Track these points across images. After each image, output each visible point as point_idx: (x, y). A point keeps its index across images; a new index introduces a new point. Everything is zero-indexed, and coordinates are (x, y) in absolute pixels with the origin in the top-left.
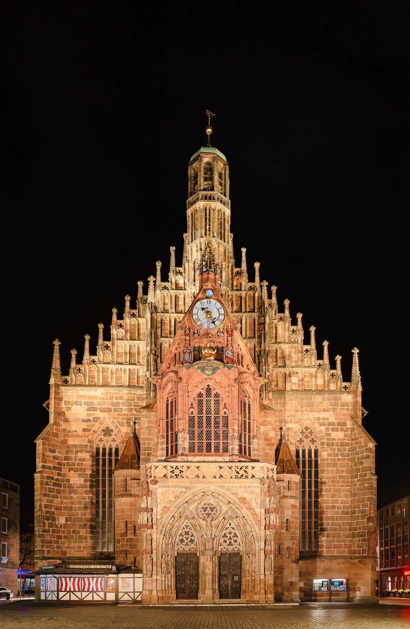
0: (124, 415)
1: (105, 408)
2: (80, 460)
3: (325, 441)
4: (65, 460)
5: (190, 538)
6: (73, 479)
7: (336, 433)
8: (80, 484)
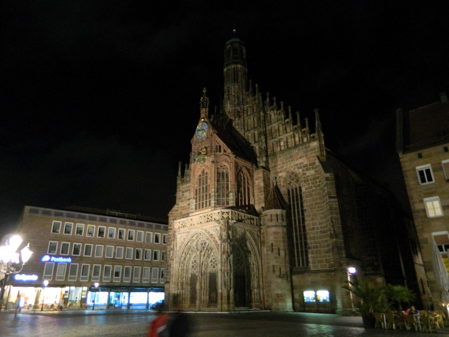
3: (303, 179)
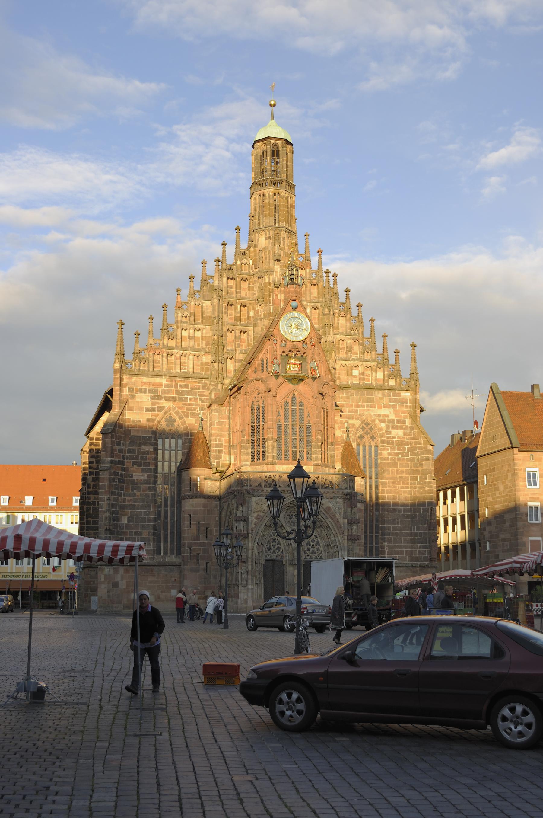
0: (190, 405)
1: (170, 397)
2: (144, 453)
3: (386, 438)
4: (128, 453)
5: (273, 549)
6: (137, 474)
7: (396, 431)
8: (144, 480)
